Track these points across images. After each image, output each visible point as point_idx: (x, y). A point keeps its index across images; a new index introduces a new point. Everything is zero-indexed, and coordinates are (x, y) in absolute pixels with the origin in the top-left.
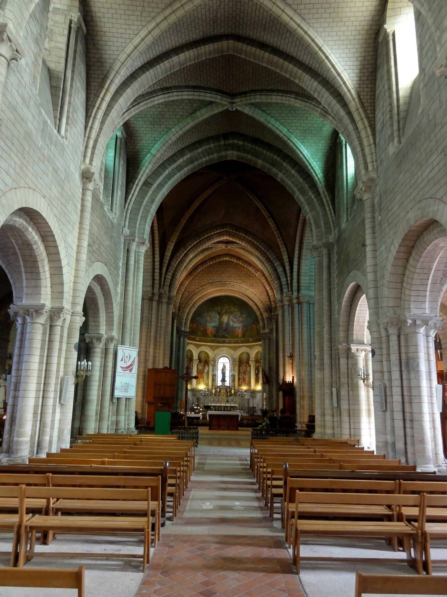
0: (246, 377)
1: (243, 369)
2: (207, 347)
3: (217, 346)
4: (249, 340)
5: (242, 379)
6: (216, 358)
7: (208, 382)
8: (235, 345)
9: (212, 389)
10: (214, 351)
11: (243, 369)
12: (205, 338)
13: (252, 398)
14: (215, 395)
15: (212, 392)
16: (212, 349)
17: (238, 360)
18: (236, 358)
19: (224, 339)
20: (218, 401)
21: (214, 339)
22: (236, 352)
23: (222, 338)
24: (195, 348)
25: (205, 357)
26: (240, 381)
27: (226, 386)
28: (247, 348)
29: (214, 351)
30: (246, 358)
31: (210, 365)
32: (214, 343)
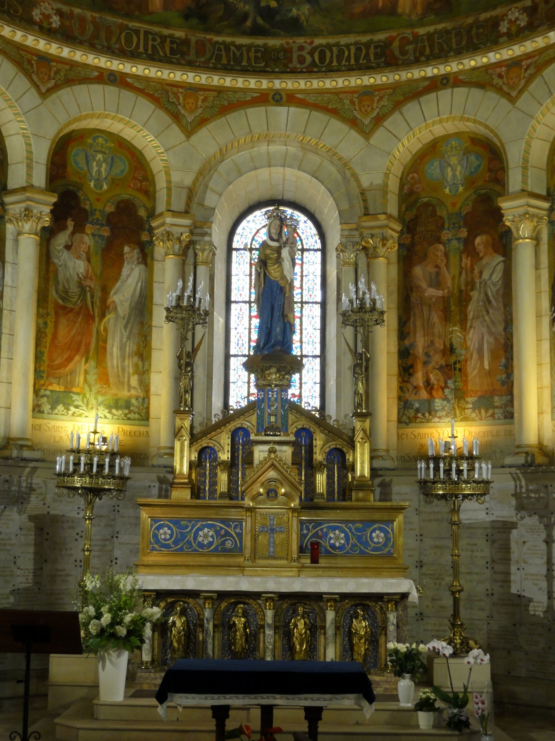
0: (473, 339)
1: (437, 282)
2: (128, 96)
3: (220, 91)
4: (495, 23)
5: (437, 359)
6: (210, 200)
7: (145, 387)
8: (368, 80)
9: (176, 433)
10: (189, 132)
11: (437, 282)
12: (110, 19)
13: (532, 521)
14: (196, 493)
15: (171, 469)
16: (176, 117)
17: (393, 208)
18: (384, 189)
19: (273, 42)
20: (222, 551)
21: (196, 37)
22: (379, 135)
23: (256, 31)
24: (22, 83)
25: (114, 183)
26: (419, 378)
27: (296, 408)
28: (476, 92)
29: (189, 132)
30: (469, 182)
31: (159, 249)
32: (191, 65)
